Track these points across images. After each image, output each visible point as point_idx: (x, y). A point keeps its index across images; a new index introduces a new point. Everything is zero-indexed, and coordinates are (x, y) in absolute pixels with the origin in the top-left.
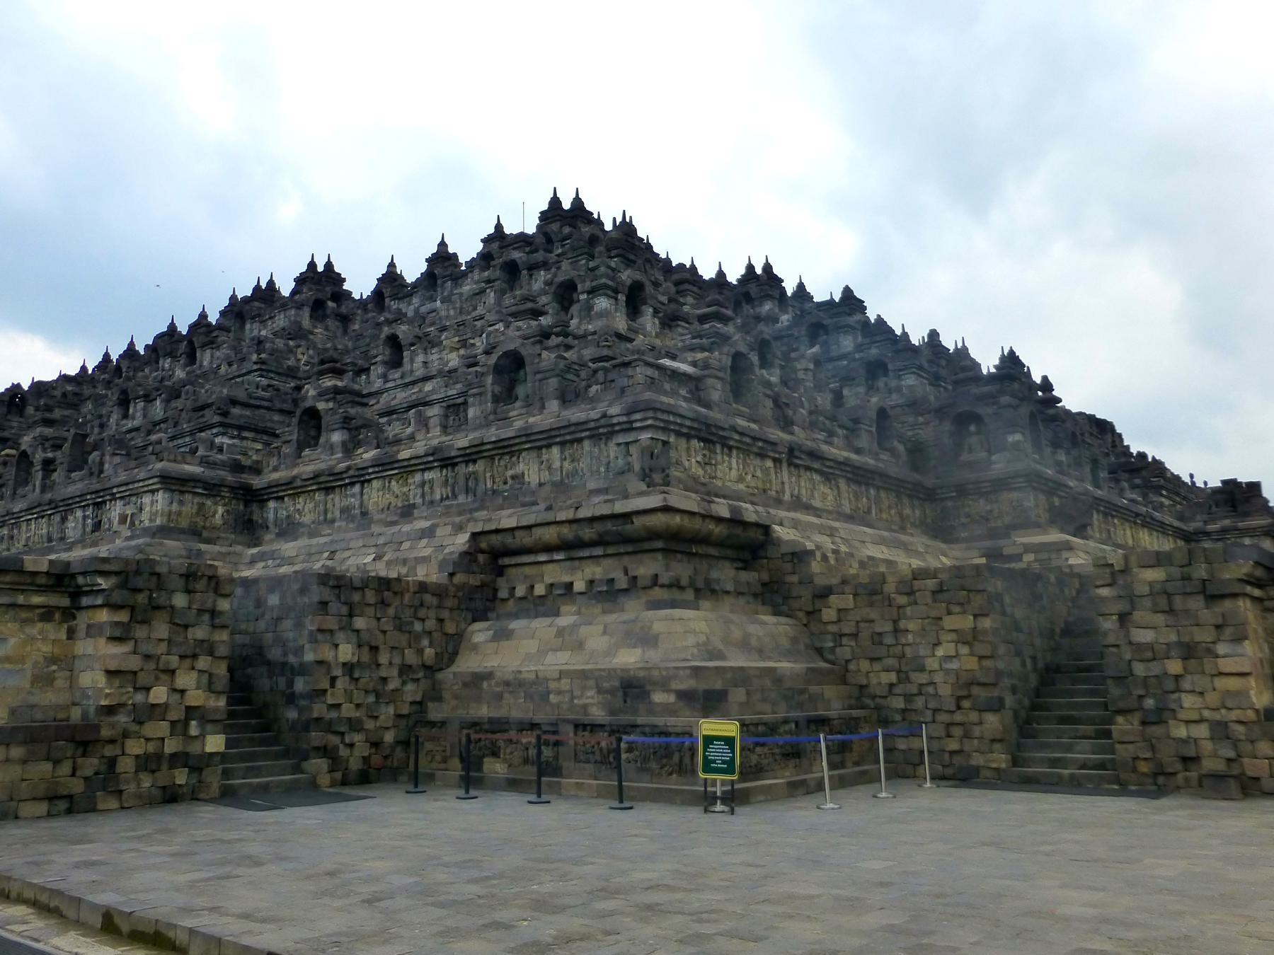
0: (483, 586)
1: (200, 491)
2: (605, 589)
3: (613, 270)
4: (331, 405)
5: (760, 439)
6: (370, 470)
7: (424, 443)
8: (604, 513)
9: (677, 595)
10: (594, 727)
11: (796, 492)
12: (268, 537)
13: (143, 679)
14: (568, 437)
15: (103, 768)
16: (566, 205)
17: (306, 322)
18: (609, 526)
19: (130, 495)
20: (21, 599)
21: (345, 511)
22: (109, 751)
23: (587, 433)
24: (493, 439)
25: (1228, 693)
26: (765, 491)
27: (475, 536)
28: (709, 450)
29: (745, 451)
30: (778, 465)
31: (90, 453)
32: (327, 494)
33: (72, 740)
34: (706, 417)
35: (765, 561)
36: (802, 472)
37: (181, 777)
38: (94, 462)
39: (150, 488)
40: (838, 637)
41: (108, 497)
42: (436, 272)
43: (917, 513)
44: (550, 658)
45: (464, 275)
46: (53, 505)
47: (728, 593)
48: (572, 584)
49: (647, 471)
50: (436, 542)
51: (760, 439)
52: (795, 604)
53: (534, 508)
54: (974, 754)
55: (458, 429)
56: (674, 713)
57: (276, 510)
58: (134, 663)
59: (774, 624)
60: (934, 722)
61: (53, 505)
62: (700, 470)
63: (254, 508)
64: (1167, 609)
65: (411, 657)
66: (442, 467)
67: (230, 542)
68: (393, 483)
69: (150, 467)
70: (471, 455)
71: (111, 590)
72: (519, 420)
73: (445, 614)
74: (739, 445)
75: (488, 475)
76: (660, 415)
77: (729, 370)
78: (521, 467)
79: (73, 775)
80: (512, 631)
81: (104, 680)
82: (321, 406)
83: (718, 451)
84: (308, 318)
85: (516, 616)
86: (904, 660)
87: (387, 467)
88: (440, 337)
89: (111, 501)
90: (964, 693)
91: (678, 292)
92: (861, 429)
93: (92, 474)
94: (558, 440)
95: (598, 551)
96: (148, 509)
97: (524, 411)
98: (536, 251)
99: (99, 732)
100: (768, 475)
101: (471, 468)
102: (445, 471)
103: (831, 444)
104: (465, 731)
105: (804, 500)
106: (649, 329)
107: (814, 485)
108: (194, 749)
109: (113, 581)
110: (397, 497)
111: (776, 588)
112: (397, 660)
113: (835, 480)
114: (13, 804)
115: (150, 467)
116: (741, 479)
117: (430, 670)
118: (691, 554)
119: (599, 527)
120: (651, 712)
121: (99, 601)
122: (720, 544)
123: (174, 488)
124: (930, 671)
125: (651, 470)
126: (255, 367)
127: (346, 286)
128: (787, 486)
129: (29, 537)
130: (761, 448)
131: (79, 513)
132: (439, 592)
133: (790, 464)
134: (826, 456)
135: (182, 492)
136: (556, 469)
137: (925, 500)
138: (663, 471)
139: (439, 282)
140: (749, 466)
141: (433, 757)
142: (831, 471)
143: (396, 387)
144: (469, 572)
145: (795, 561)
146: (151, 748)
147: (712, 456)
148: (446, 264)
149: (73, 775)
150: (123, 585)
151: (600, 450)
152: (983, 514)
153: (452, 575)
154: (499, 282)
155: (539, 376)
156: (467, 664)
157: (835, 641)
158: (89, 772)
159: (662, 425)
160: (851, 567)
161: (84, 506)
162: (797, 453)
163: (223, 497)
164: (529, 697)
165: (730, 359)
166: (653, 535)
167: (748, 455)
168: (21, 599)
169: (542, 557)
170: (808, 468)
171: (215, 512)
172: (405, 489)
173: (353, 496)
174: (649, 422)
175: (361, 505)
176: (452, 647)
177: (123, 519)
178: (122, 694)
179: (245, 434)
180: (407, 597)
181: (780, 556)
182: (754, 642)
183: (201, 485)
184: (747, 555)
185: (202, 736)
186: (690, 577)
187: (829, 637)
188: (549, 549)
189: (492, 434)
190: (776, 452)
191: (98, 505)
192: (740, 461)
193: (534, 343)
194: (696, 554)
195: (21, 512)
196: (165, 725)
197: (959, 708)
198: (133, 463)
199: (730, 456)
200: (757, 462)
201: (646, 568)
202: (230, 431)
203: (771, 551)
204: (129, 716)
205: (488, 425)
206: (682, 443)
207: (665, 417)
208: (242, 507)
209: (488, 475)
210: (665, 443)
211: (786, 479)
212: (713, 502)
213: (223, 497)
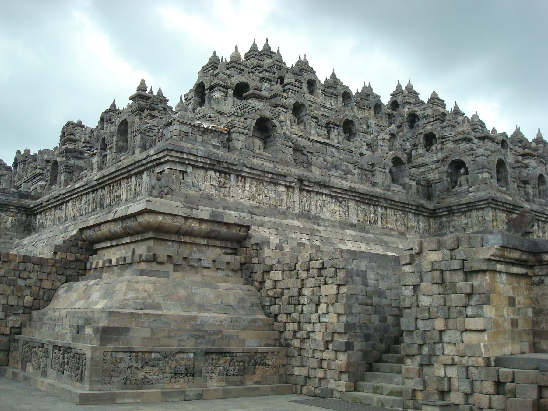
0: (77, 260)
3: (229, 76)
16: (260, 49)
25: (470, 346)
26: (275, 206)
30: (290, 190)
32: (56, 210)
35: (245, 249)
36: (313, 195)
40: (273, 299)
43: (422, 225)
54: (331, 380)
60: (313, 357)
63: (32, 219)
64: (439, 281)
65: (13, 301)
76: (173, 154)
77: (252, 129)
82: (59, 160)
83: (232, 179)
86: (302, 315)
90: (329, 339)
92: (376, 170)
100: (280, 196)
103: (346, 179)
105: (313, 213)
113: (345, 202)
122: (207, 236)
124: (314, 323)
127: (169, 104)
128: (297, 204)
130: (271, 178)
132: (41, 262)
133: (301, 190)
134: (331, 185)
137: (429, 217)
142: (340, 195)
145: (258, 249)
147: (227, 181)
152: (463, 226)
153: (55, 253)
159: (178, 160)
162: (305, 183)
163: (12, 212)
166: (147, 228)
170: (317, 193)
171: (7, 219)
172: (80, 206)
174: (167, 158)
182: (197, 300)
184: (235, 245)
194: (185, 243)
197: (327, 348)
200: (272, 187)
203: (248, 243)
206: (201, 173)
207: (179, 155)
208: (24, 218)
209: (108, 195)
210: (184, 173)
211: (297, 199)
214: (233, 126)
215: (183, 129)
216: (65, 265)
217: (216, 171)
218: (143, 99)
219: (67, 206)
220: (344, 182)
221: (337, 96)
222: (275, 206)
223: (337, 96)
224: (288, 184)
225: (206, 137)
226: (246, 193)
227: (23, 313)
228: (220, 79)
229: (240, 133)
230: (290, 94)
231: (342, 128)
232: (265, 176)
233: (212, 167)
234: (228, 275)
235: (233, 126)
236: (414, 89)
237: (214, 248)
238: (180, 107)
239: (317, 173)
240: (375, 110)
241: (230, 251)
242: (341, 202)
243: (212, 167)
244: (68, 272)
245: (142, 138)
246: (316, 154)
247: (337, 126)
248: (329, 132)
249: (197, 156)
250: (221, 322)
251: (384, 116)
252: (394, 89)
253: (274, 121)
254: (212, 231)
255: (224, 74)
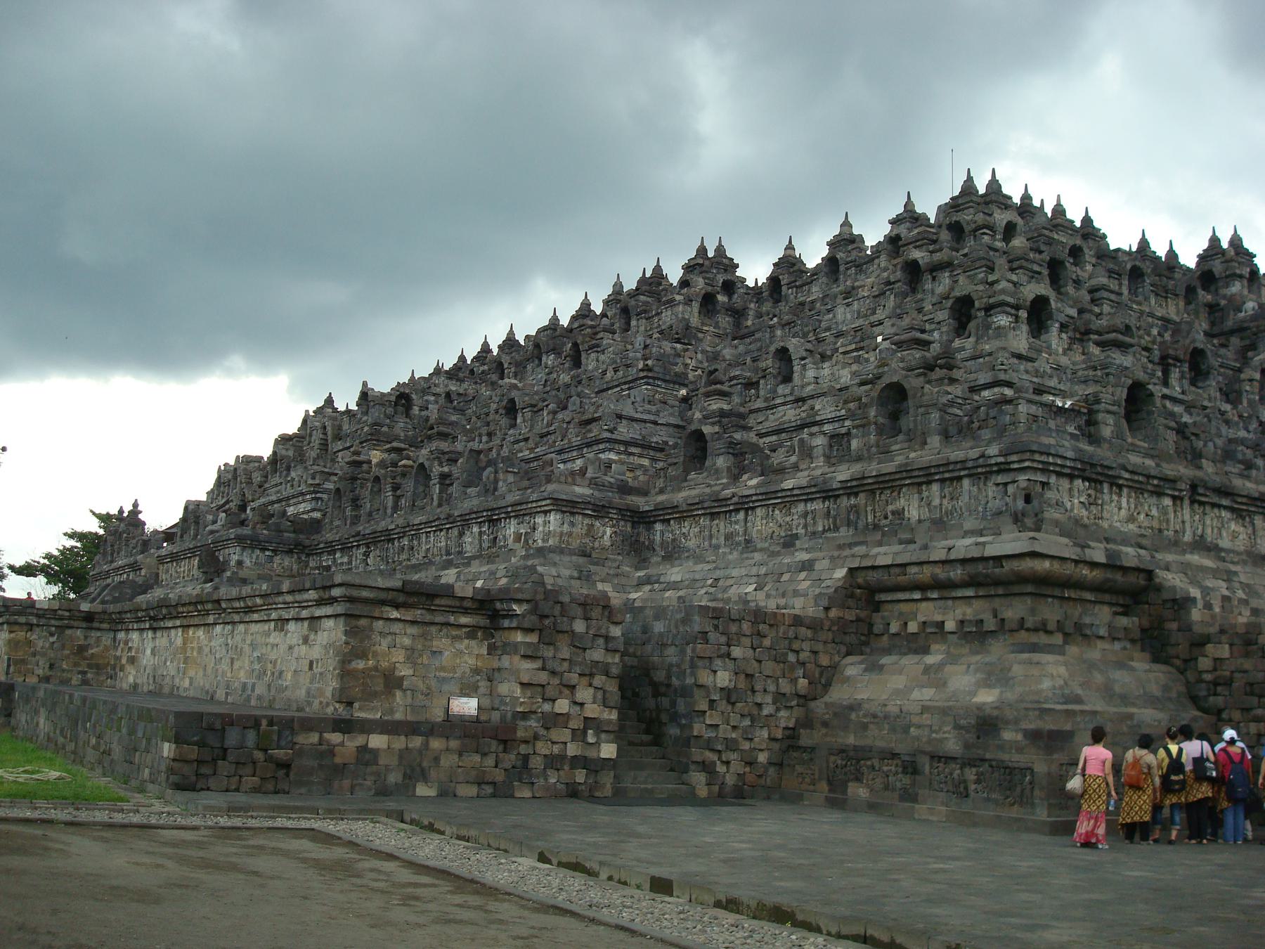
0: (858, 620)
1: (589, 512)
2: (974, 629)
3: (1015, 284)
4: (717, 429)
5: (1154, 477)
6: (754, 498)
7: (806, 473)
8: (975, 556)
9: (1042, 639)
10: (949, 759)
11: (1199, 532)
12: (655, 559)
13: (550, 692)
14: (947, 475)
15: (519, 763)
16: (982, 190)
17: (695, 320)
18: (980, 568)
19: (524, 515)
20: (452, 619)
21: (729, 537)
22: (523, 749)
23: (966, 472)
24: (874, 474)
26: (1160, 531)
27: (851, 570)
28: (1095, 489)
29: (1138, 489)
30: (1178, 502)
31: (484, 469)
32: (712, 520)
33: (495, 738)
34: (1091, 456)
35: (1147, 606)
36: (1208, 508)
37: (580, 776)
38: (488, 478)
39: (543, 509)
40: (1212, 687)
41: (503, 515)
42: (838, 256)
44: (916, 694)
45: (871, 260)
46: (451, 520)
47: (1102, 638)
48: (943, 622)
49: (1020, 515)
50: (814, 575)
51: (1154, 477)
52: (1172, 651)
53: (912, 547)
55: (841, 460)
56: (1020, 750)
57: (662, 533)
58: (543, 677)
59: (1146, 671)
61: (451, 520)
62: (1084, 511)
63: (641, 530)
65: (785, 687)
66: (824, 499)
67: (618, 563)
68: (777, 512)
69: (543, 489)
70: (850, 489)
71: (523, 616)
72: (903, 455)
73: (820, 647)
74: (1130, 484)
75: (869, 509)
76: (1037, 457)
77: (1124, 403)
78: (902, 503)
79: (496, 767)
80: (882, 666)
81: (519, 691)
82: (707, 430)
83: (1105, 491)
84: (696, 315)
85: (887, 651)
87: (771, 498)
88: (836, 343)
89: (505, 518)
91: (1093, 301)
93: (487, 491)
94: (937, 477)
95: (970, 592)
96: (541, 529)
97: (906, 445)
98: (941, 250)
99: (515, 732)
100: (1166, 513)
101: (853, 501)
102: (827, 503)
103: (1248, 477)
104: (832, 758)
105: (1209, 539)
106: (1054, 346)
107: (1222, 523)
108: (591, 754)
109: (525, 607)
110: (780, 526)
111: (1156, 634)
112: (772, 688)
113: (1250, 517)
114: (452, 785)
115: (543, 489)
116: (1131, 519)
117: (804, 699)
118: (1062, 598)
119: (971, 569)
120: (1001, 748)
121: (514, 625)
123: (564, 509)
125: (1023, 515)
126: (642, 374)
127: (739, 273)
128: (1188, 525)
129: (428, 549)
131: (476, 529)
132: (815, 625)
133: (1192, 502)
134: (1236, 492)
135: (573, 514)
136: (935, 507)
138: (1036, 515)
139: (842, 268)
140: (1142, 505)
141: (804, 778)
142: (1244, 507)
143: (784, 404)
144: (843, 606)
145: (1176, 608)
146: (556, 749)
148: (850, 248)
149: (496, 767)
150: (534, 611)
151: (979, 489)
153: (827, 609)
154: (900, 284)
155: (921, 410)
156: (839, 694)
157: (1209, 690)
158: (508, 765)
159: (1040, 466)
160: (1240, 614)
161: (481, 522)
162: (1201, 491)
163: (611, 519)
164: (893, 730)
165: (1126, 391)
166: (1022, 579)
167: (1142, 494)
168: (452, 619)
169: (917, 596)
170: (1214, 505)
171: (605, 533)
172: (788, 519)
173: (736, 523)
174: (1027, 464)
175: (746, 531)
176: (825, 679)
177: (518, 538)
178: (533, 703)
179: (633, 450)
180: (782, 629)
181: (1160, 602)
182: (1117, 689)
183: (591, 507)
184: (1128, 601)
185: (598, 744)
186: (1058, 621)
187: (1203, 685)
188: (922, 587)
189: (873, 468)
190: (1175, 489)
191: (492, 522)
192: (1132, 500)
193: (919, 375)
194: (1069, 599)
195: (420, 524)
196: (568, 732)
198: (526, 483)
199: (1120, 496)
200: (1154, 500)
201: (1014, 610)
202: (616, 446)
204: (538, 722)
205: (870, 458)
206: (1065, 483)
207: (1043, 458)
208: (629, 529)
209: (869, 509)
210: (1044, 484)
211: (1187, 517)
212: (1089, 547)
213: (611, 519)
214: (1098, 402)
215: (1031, 411)
216: (842, 626)
217: (1084, 479)
218: (918, 344)
219: (747, 514)
220: (1249, 485)
221: (1120, 275)
222: (1160, 531)
223: (1120, 275)
224: (1177, 493)
225: (1061, 420)
226: (1123, 512)
227: (798, 705)
228: (1003, 291)
229: (1109, 412)
230: (1106, 308)
231: (1187, 365)
232: (1148, 483)
233: (1081, 474)
234: (1125, 648)
235: (1098, 402)
236: (1246, 245)
237: (1101, 606)
238: (895, 328)
239: (1210, 470)
240: (1186, 297)
241: (1121, 610)
242: (1244, 519)
243: (1081, 474)
244: (848, 639)
245: (941, 418)
246: (1202, 436)
247: (1180, 361)
248: (1166, 373)
249: (1065, 458)
250: (1160, 722)
251: (1202, 310)
252: (1206, 245)
253: (1150, 387)
254: (1107, 580)
255: (1009, 281)
